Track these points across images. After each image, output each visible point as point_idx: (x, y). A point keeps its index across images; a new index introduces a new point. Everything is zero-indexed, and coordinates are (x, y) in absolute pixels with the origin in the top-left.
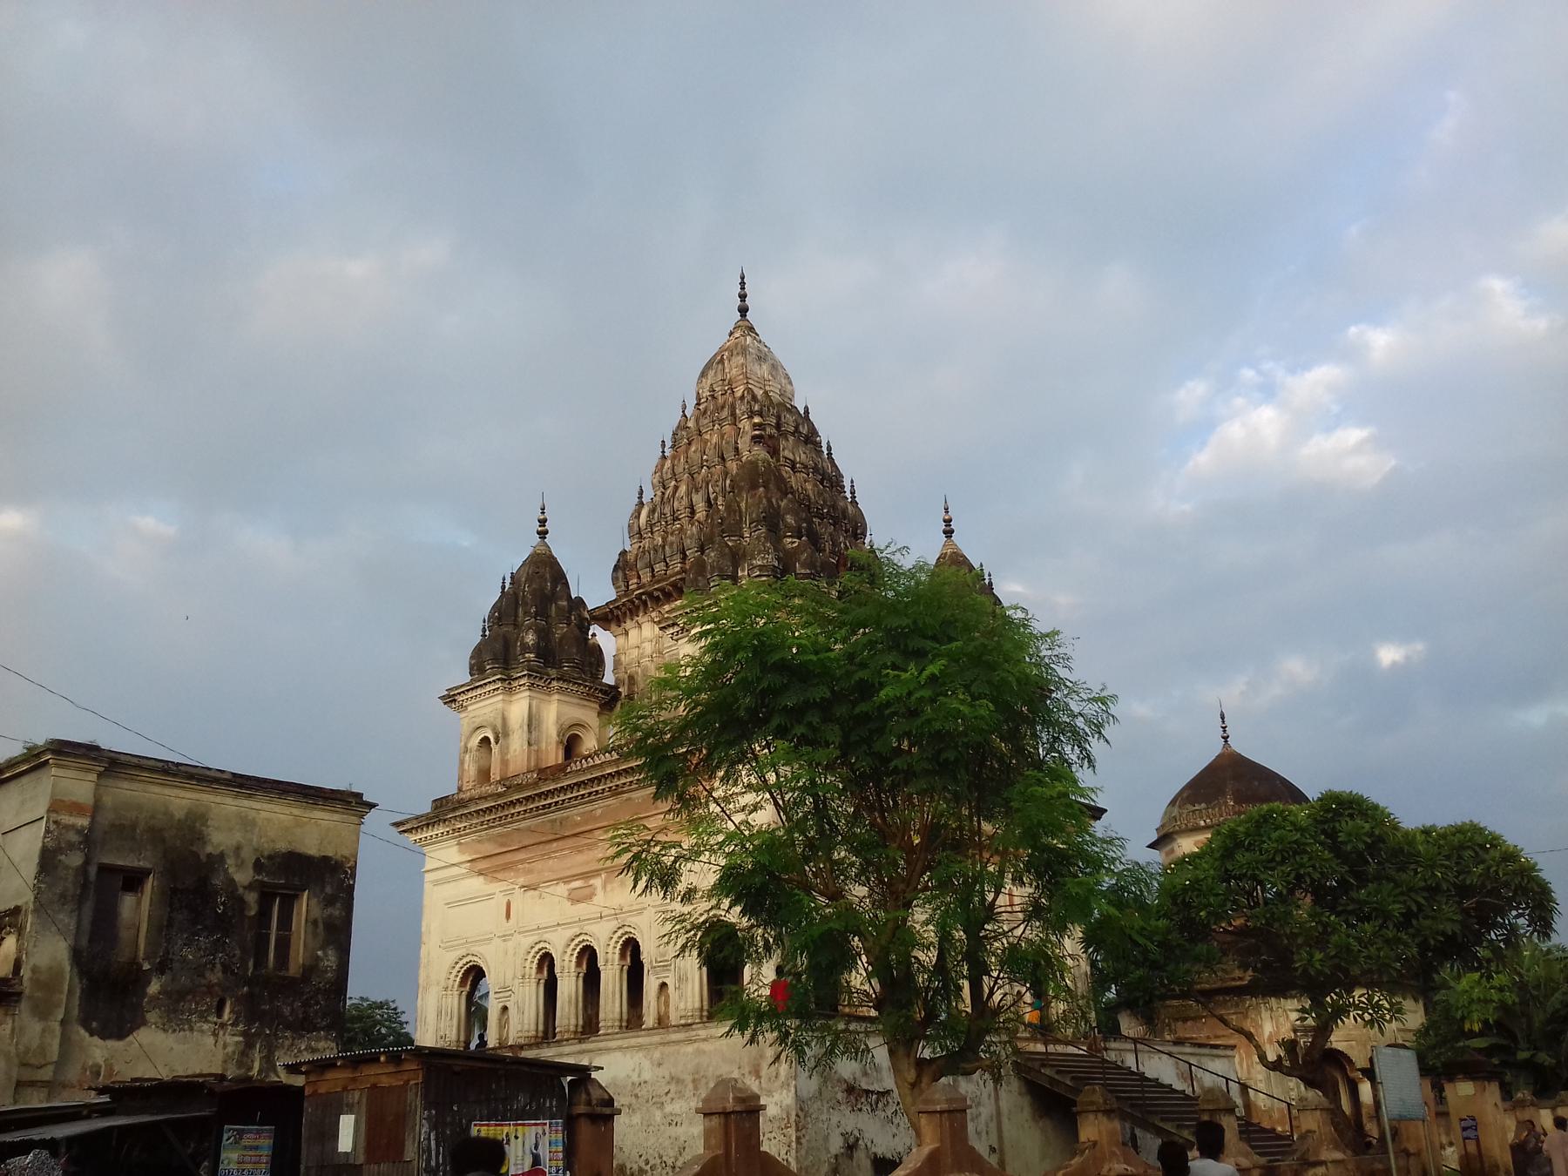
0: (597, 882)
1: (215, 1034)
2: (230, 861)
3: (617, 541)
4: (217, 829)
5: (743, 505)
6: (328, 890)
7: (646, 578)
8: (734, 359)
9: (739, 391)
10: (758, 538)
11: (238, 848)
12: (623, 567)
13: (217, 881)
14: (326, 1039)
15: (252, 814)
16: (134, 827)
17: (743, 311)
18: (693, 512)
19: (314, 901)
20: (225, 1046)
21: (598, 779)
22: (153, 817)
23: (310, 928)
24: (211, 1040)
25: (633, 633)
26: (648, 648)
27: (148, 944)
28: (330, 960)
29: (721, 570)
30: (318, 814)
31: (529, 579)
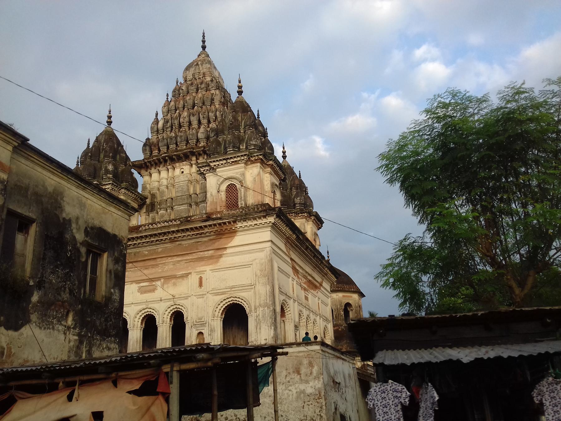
0: (159, 283)
1: (65, 334)
2: (74, 225)
3: (145, 133)
4: (68, 204)
5: (240, 118)
6: (116, 254)
7: (164, 149)
8: (204, 65)
9: (208, 79)
10: (252, 132)
11: (77, 218)
12: (148, 145)
13: (68, 236)
14: (115, 343)
15: (84, 200)
16: (27, 189)
17: (204, 47)
18: (190, 123)
19: (110, 259)
20: (69, 342)
21: (165, 234)
22: (37, 186)
23: (108, 275)
24: (62, 337)
25: (155, 176)
26: (165, 182)
27: (33, 269)
28: (116, 297)
29: (234, 144)
30: (113, 209)
31: (106, 141)
